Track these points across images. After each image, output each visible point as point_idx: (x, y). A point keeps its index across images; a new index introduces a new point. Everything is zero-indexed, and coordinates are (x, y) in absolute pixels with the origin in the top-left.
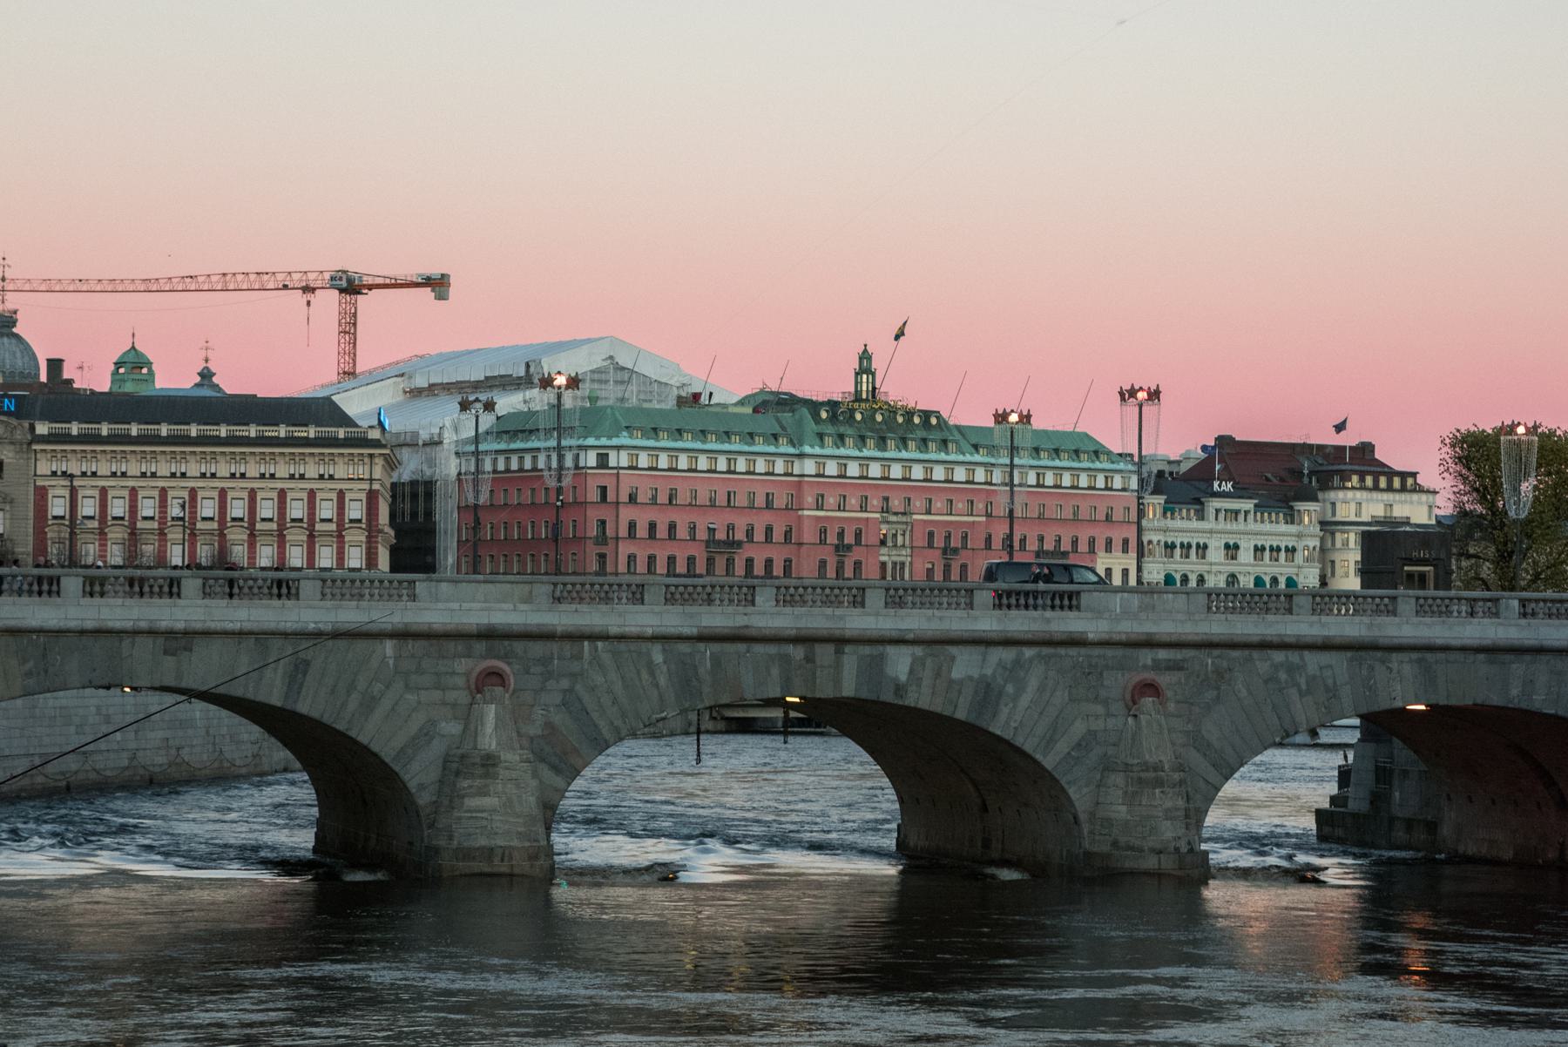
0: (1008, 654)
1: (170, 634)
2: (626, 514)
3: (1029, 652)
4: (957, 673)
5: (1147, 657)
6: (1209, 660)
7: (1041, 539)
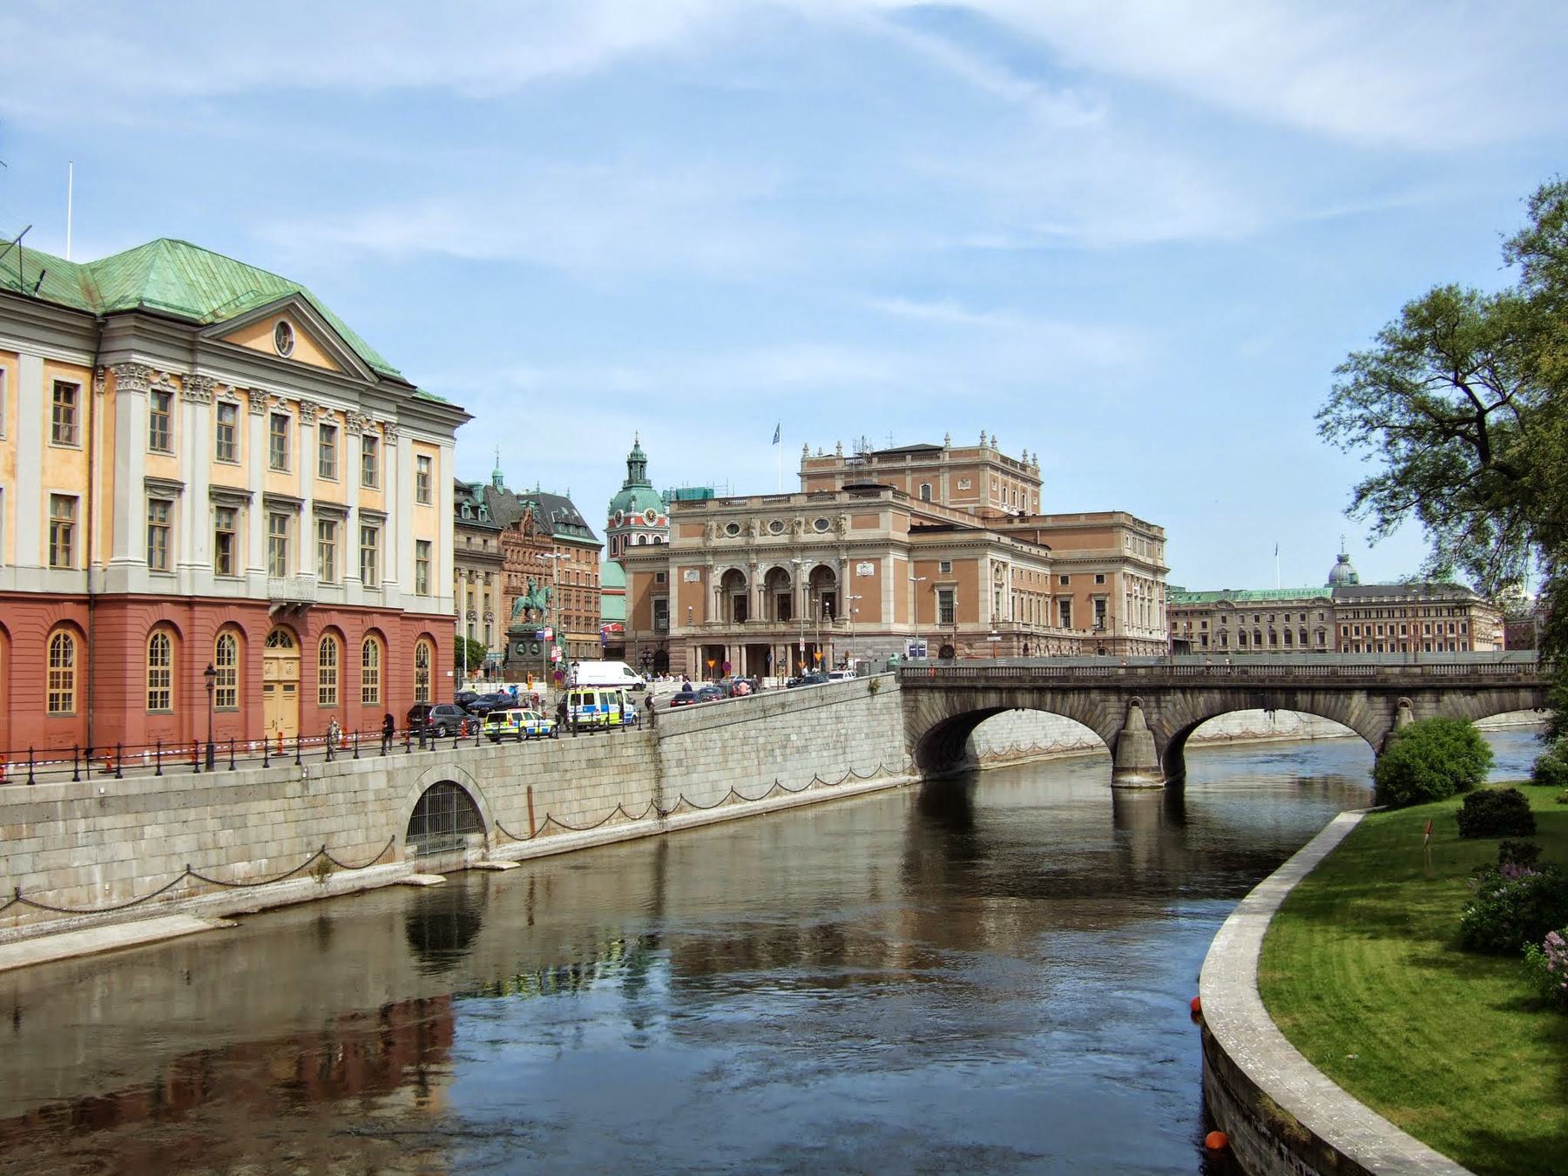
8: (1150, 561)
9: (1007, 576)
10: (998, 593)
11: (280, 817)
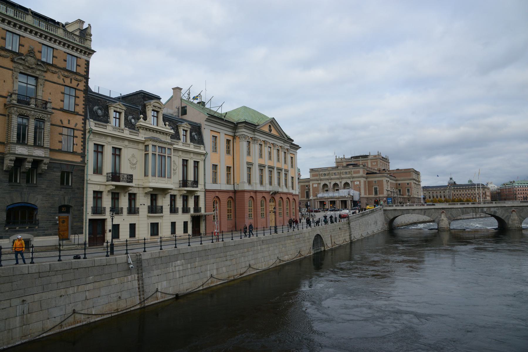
0: (497, 208)
1: (413, 209)
2: (518, 192)
3: (499, 208)
4: (491, 210)
5: (513, 208)
6: (521, 208)
8: (417, 179)
9: (389, 184)
11: (292, 244)
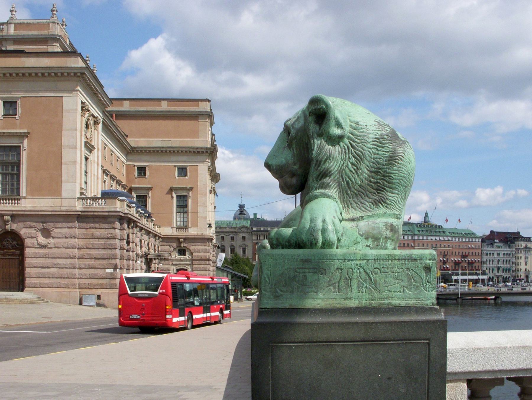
7: (462, 253)
10: (87, 159)
